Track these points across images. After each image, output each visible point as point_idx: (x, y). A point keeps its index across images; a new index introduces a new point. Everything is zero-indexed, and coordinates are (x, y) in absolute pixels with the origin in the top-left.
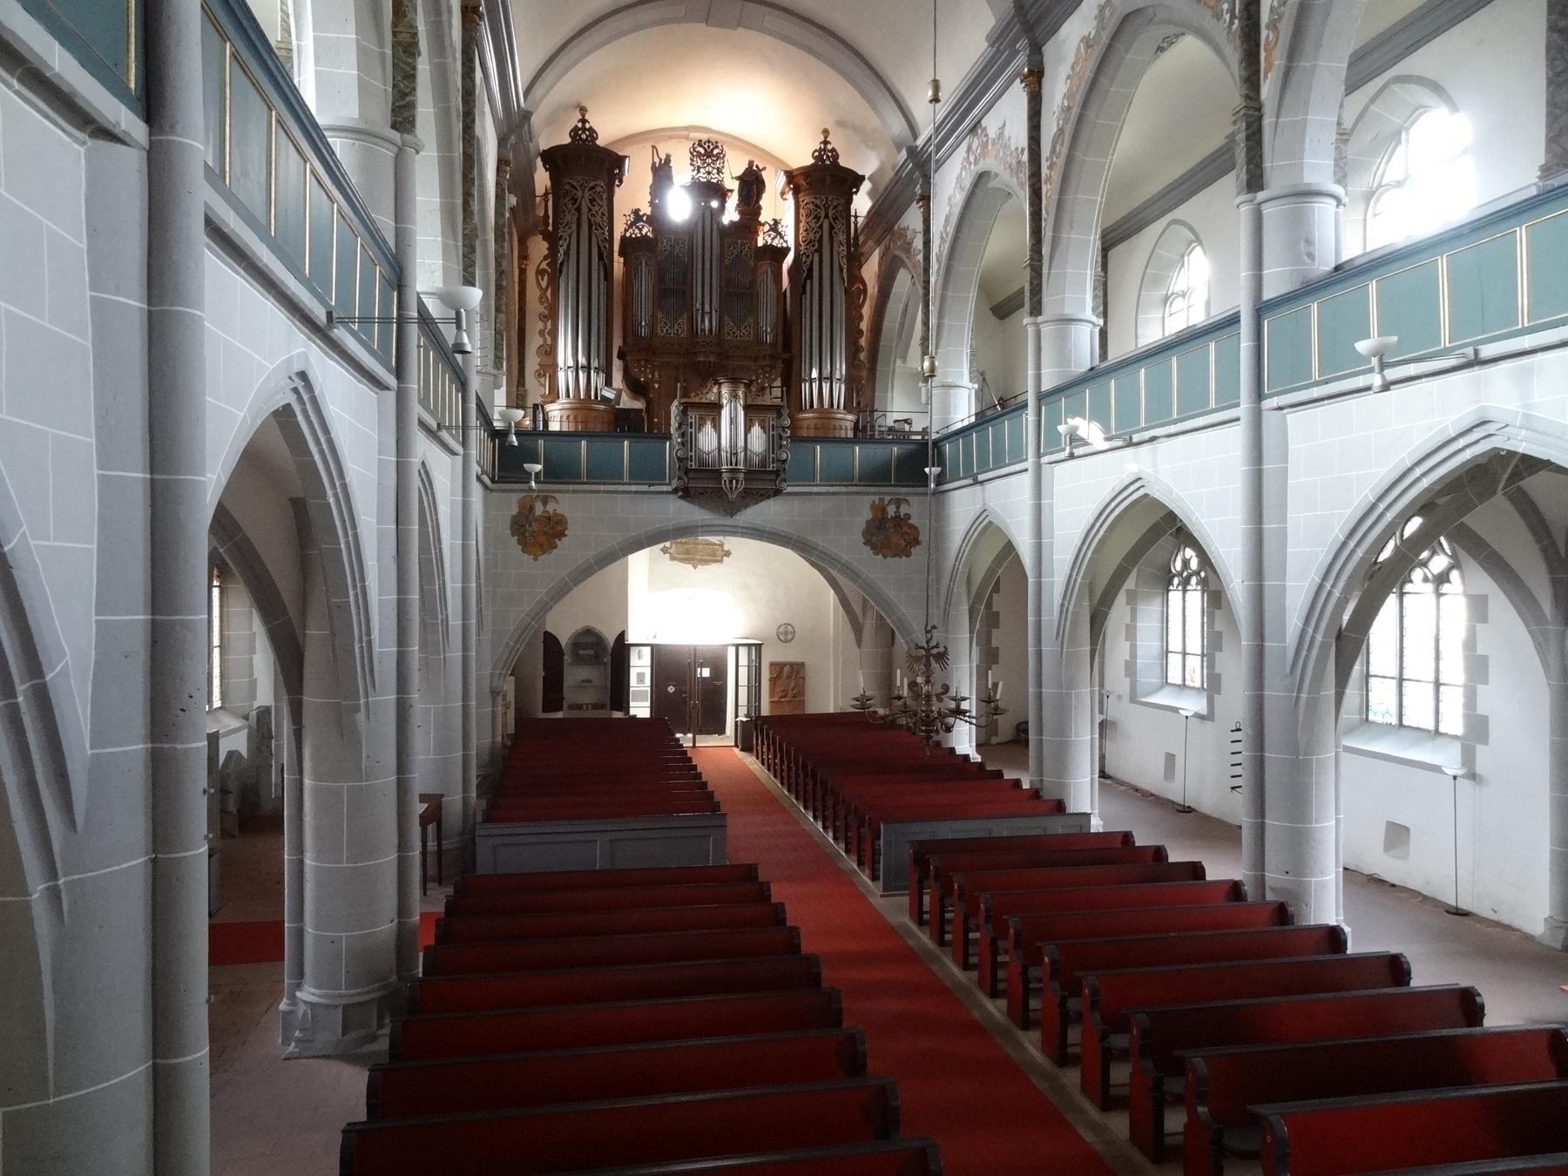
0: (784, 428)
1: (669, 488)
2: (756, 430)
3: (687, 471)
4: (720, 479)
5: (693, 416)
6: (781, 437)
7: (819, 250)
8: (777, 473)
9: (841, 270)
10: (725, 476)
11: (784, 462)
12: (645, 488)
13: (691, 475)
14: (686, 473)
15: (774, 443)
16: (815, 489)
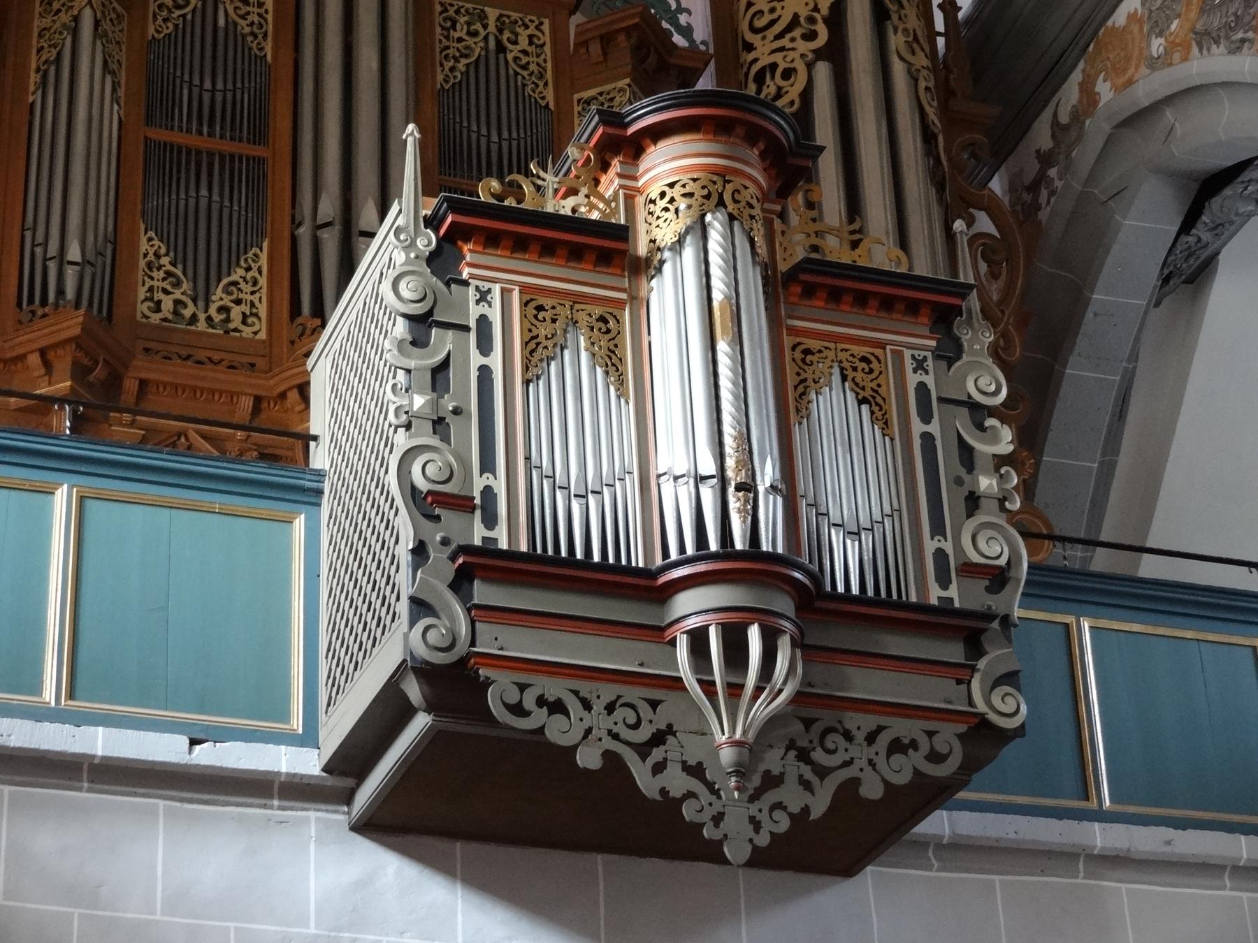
0: (978, 412)
1: (308, 763)
2: (833, 406)
3: (476, 565)
4: (659, 634)
5: (494, 290)
6: (967, 455)
7: (836, 52)
8: (972, 630)
9: (928, 137)
10: (692, 607)
11: (998, 578)
12: (167, 748)
13: (482, 592)
14: (461, 583)
15: (933, 483)
16: (1099, 836)
